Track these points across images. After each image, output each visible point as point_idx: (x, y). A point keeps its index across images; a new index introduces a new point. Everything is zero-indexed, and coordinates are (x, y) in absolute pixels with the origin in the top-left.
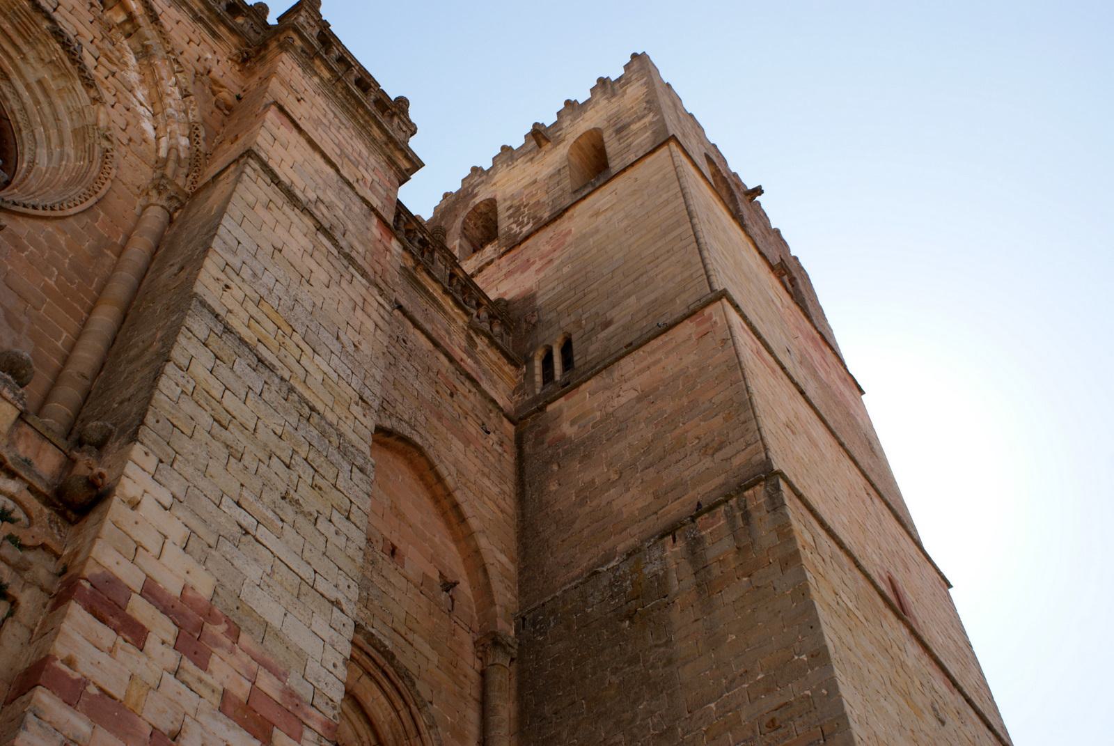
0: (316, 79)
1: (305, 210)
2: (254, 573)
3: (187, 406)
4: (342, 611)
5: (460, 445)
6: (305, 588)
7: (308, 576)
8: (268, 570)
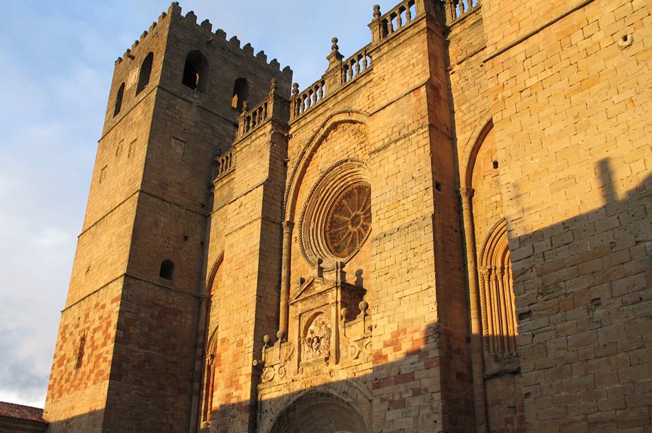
0: (384, 56)
1: (389, 145)
3: (379, 280)
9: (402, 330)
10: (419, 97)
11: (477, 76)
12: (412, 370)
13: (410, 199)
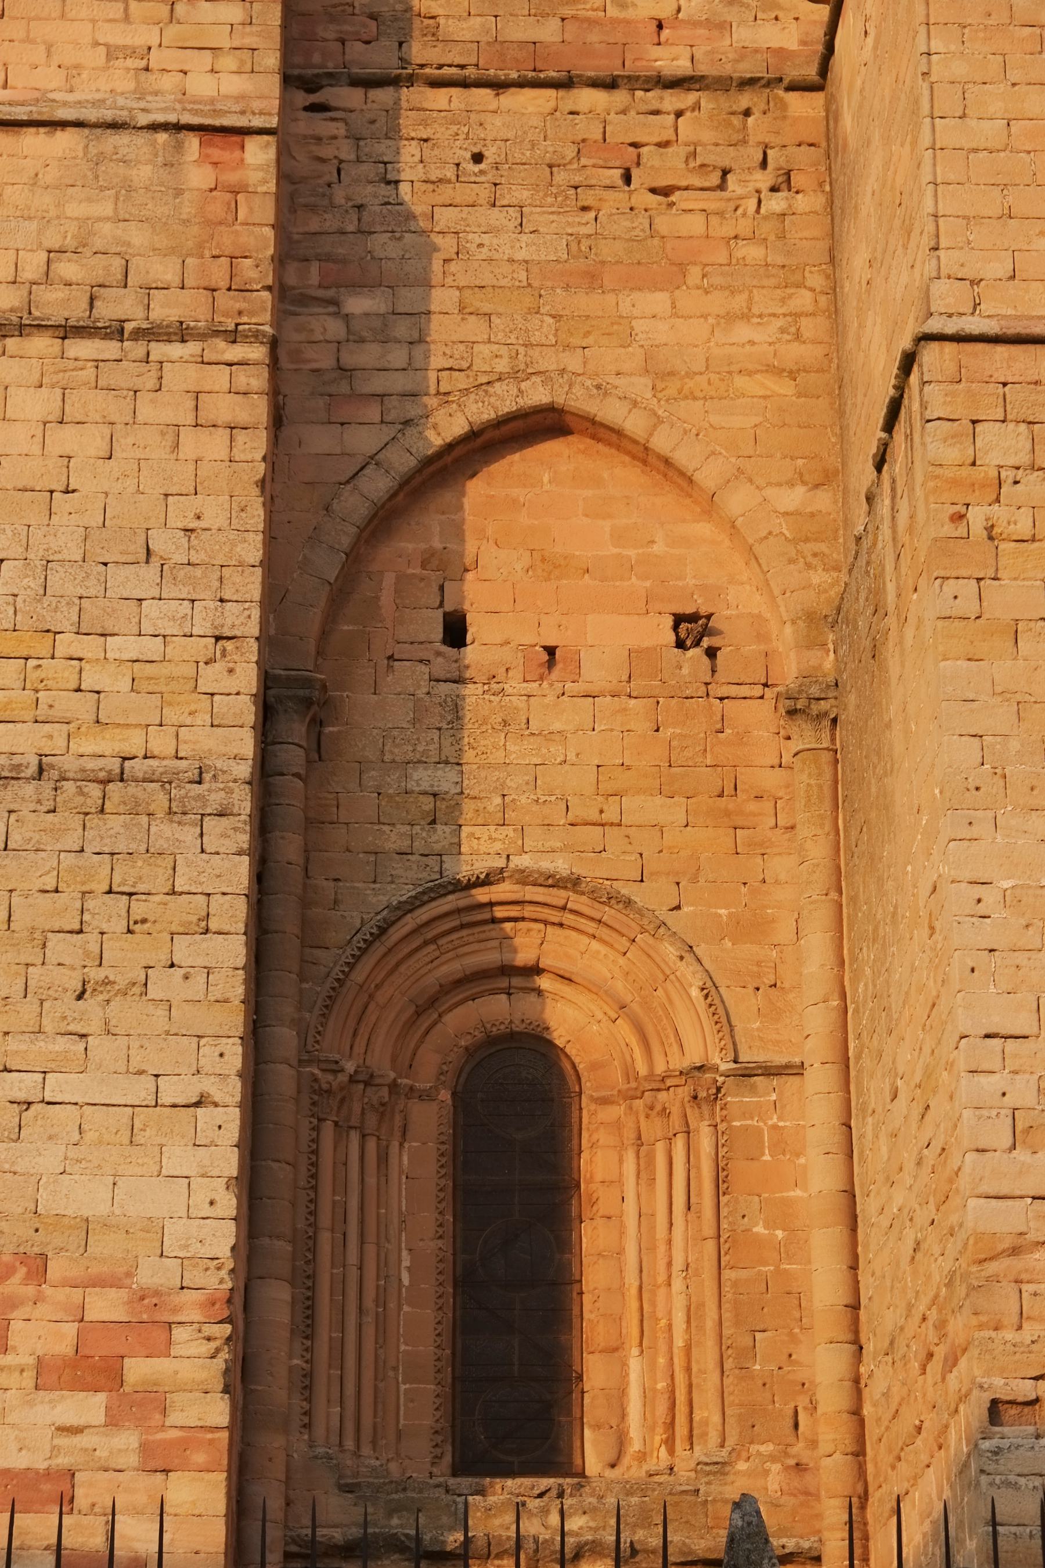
2: (50, 1159)
4: (216, 1105)
5: (658, 301)
6: (142, 1115)
7: (143, 1094)
8: (76, 1137)
9: (23, 1258)
10: (232, 177)
11: (446, 193)
12: (63, 1461)
13: (124, 647)
